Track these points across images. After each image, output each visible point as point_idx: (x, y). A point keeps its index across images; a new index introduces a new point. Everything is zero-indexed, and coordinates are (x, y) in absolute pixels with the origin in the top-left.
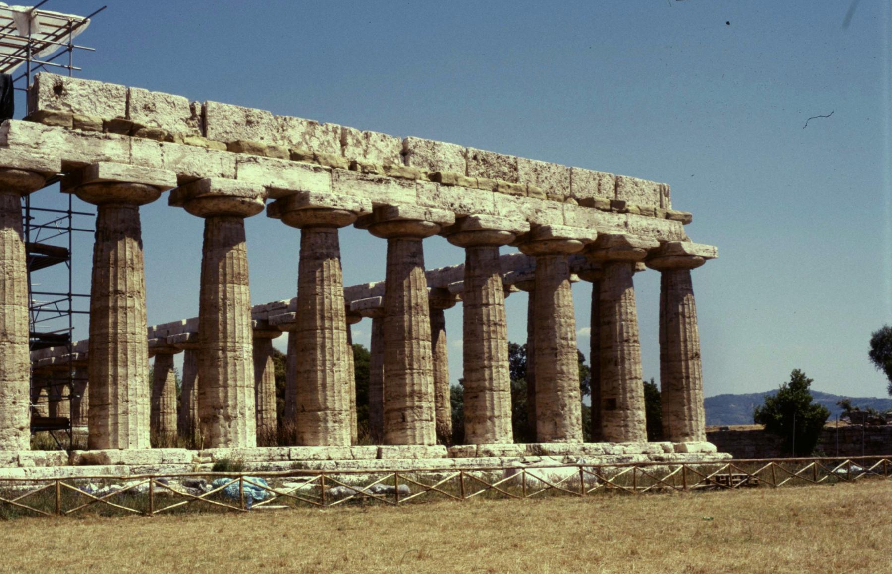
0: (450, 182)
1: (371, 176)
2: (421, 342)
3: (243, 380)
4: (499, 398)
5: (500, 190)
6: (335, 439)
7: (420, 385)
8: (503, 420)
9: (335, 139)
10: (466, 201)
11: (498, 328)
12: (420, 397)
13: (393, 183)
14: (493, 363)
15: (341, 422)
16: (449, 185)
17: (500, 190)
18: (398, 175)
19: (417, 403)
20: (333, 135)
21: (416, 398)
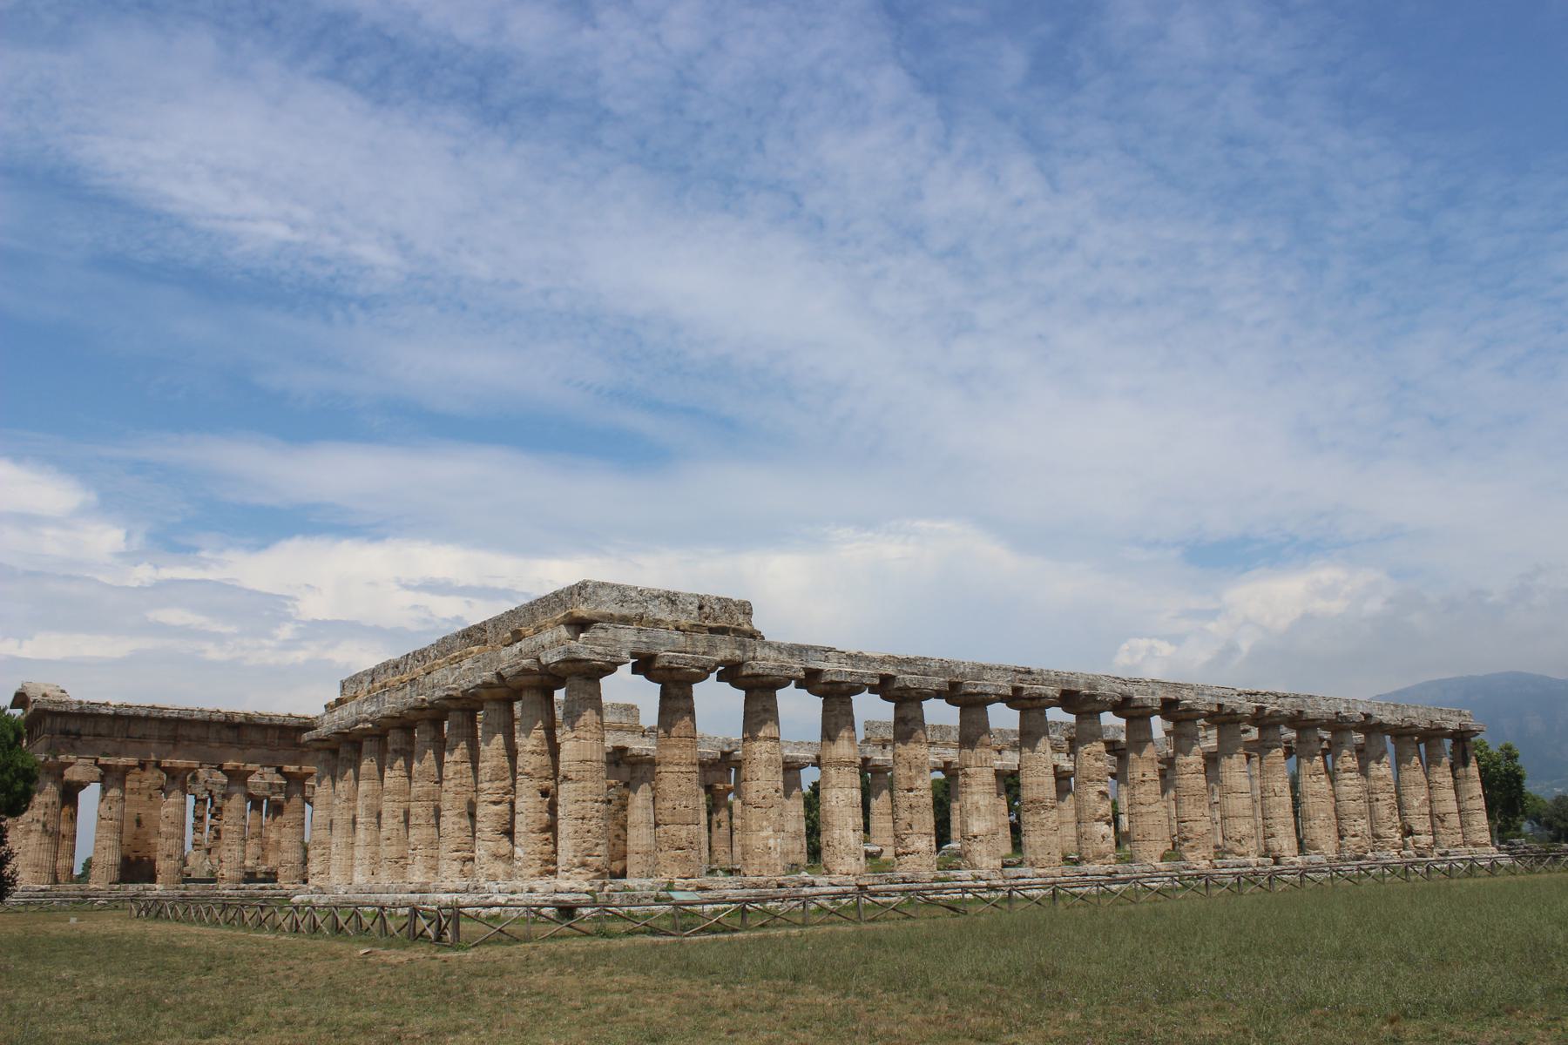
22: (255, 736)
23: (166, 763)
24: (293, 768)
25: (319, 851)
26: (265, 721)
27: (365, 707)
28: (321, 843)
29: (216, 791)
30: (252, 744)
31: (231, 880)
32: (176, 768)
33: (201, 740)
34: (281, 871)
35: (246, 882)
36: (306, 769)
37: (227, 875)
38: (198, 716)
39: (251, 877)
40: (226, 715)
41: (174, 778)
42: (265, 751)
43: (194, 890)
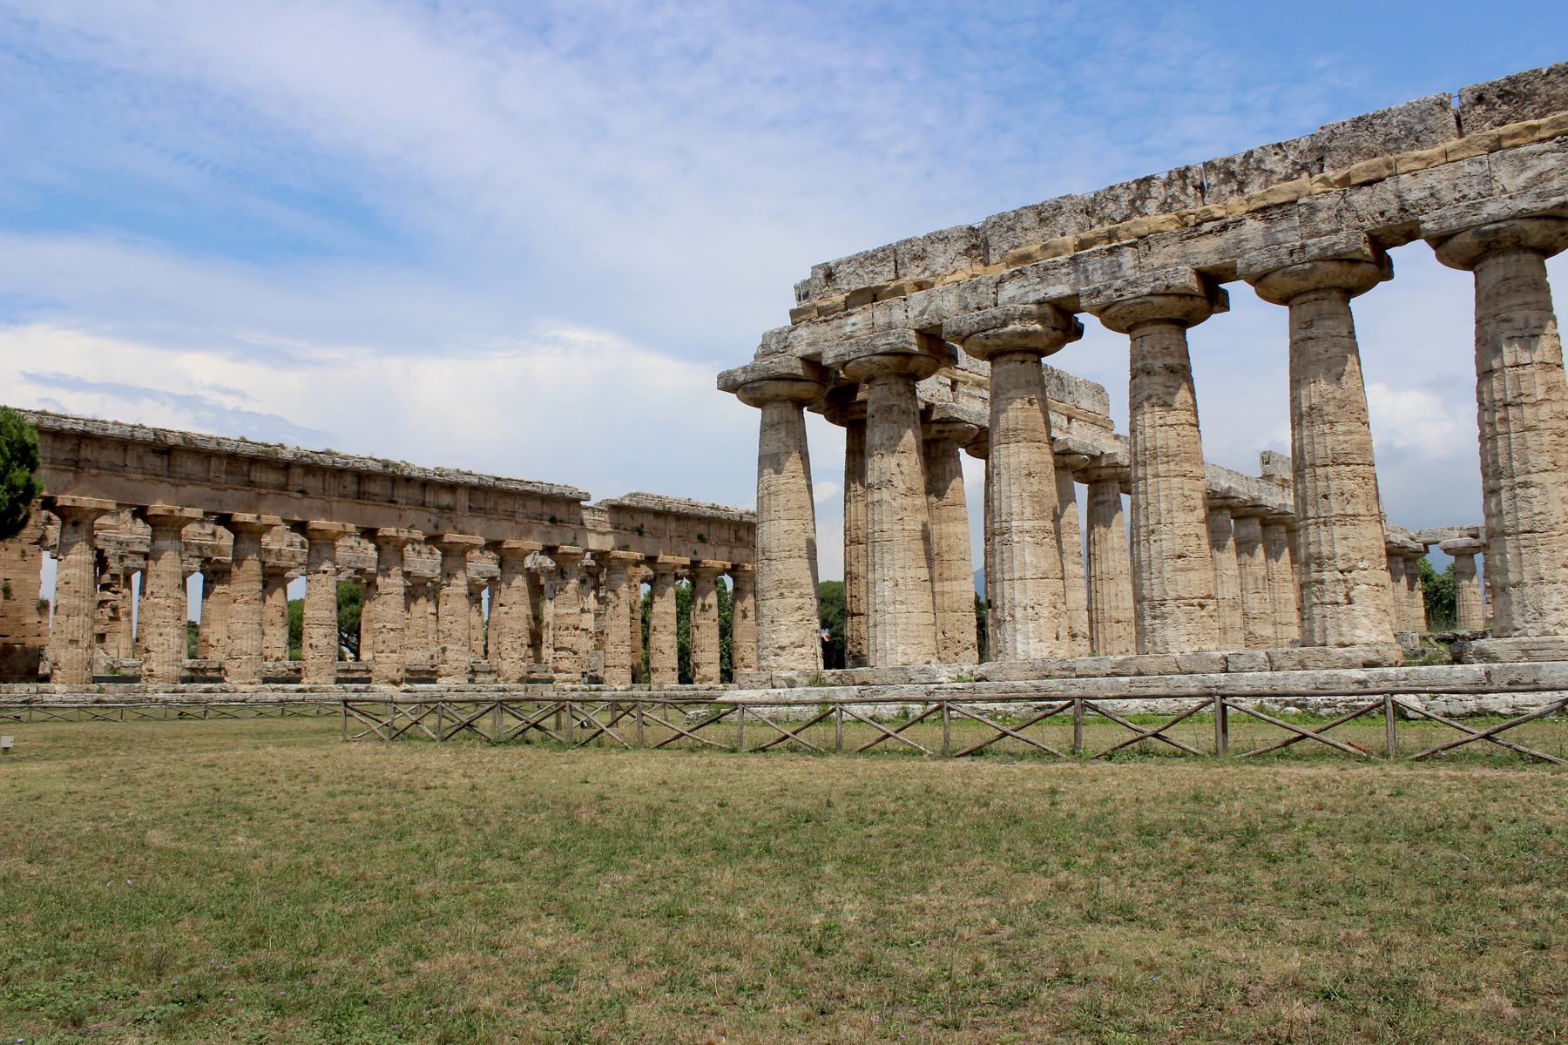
0: (1372, 176)
1: (1207, 227)
2: (1320, 471)
3: (1012, 570)
4: (1518, 547)
5: (1506, 143)
6: (1155, 644)
7: (1319, 543)
8: (1527, 590)
9: (1184, 189)
10: (1412, 197)
11: (1512, 411)
12: (1319, 565)
13: (1249, 222)
14: (1503, 482)
15: (1163, 616)
16: (1369, 183)
17: (1506, 143)
18: (1262, 204)
19: (1315, 576)
20: (1179, 183)
21: (1314, 567)
22: (191, 466)
23: (64, 500)
24: (249, 517)
25: (792, 601)
26: (212, 446)
27: (1010, 290)
28: (793, 585)
29: (110, 551)
30: (189, 479)
31: (164, 678)
32: (80, 509)
33: (115, 469)
34: (230, 666)
35: (184, 680)
36: (267, 519)
37: (158, 671)
38: (114, 431)
39: (195, 675)
40: (155, 432)
41: (76, 524)
42: (206, 491)
43: (114, 692)
